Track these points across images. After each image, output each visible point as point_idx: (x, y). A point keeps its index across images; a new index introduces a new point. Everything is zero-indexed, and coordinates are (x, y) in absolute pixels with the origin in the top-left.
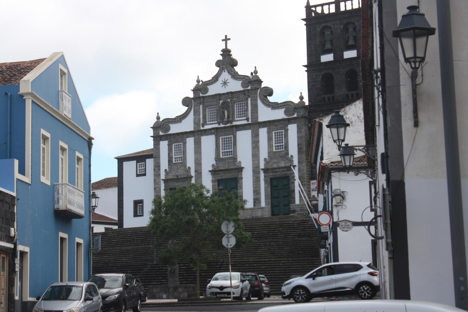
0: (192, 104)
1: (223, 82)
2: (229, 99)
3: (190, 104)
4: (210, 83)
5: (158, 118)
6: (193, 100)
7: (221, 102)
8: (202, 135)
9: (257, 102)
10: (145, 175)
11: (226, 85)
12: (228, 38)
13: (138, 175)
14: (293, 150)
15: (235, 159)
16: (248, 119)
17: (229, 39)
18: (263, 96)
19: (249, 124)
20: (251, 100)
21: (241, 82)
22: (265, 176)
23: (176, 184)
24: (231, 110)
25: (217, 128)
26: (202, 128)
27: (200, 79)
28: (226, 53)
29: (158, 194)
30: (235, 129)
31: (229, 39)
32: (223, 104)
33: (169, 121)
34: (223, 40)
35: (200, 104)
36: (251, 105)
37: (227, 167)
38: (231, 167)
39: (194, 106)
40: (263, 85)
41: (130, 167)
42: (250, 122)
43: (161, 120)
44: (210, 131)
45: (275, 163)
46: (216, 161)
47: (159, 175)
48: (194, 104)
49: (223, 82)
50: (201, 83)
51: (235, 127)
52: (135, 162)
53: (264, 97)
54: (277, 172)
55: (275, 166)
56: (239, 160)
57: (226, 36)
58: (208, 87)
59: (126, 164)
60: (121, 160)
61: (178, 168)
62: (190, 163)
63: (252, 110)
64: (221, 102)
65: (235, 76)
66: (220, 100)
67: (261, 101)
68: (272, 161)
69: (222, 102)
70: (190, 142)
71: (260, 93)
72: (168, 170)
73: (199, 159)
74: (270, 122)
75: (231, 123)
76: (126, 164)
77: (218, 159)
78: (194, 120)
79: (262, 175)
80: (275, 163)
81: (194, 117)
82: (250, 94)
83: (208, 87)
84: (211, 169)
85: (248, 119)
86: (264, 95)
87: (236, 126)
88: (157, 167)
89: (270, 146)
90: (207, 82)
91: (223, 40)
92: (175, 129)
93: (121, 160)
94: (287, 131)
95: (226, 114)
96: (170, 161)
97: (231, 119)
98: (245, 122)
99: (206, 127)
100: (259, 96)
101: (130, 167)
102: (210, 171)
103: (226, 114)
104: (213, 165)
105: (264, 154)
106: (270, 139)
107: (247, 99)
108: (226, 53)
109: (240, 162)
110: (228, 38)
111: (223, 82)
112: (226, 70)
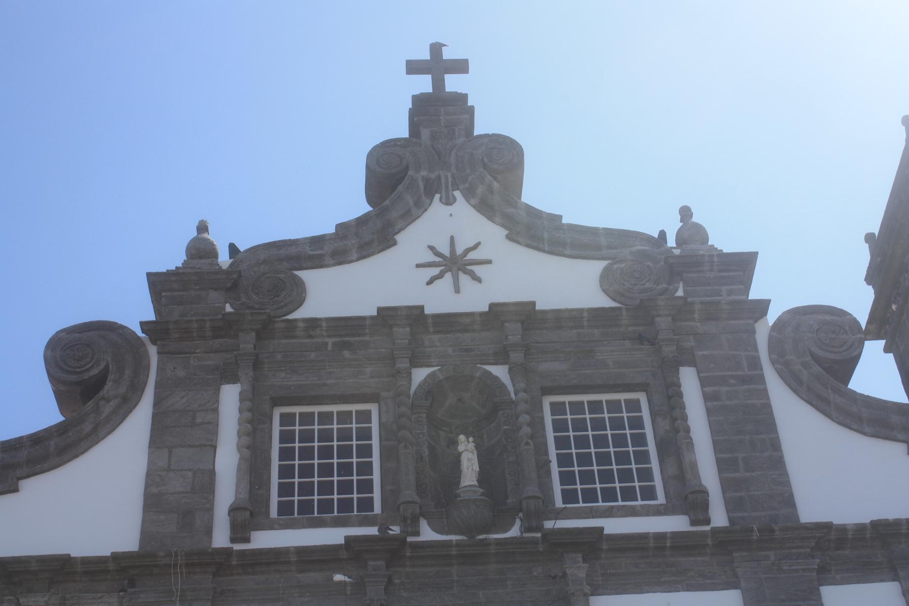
0: (141, 368)
1: (438, 254)
2: (501, 357)
3: (128, 372)
4: (321, 257)
6: (153, 350)
7: (420, 375)
9: (765, 393)
11: (464, 279)
12: (447, 54)
17: (461, 67)
18: (808, 358)
20: (704, 383)
21: (599, 266)
24: (526, 430)
27: (220, 240)
31: (461, 67)
34: (413, 68)
36: (709, 412)
39: (158, 385)
40: (772, 316)
44: (313, 577)
48: (160, 369)
49: (446, 252)
50: (224, 259)
51: (579, 557)
53: (817, 369)
58: (306, 275)
63: (718, 446)
64: (420, 375)
66: (416, 361)
67: (795, 391)
69: (431, 376)
75: (532, 522)
78: (153, 478)
81: (151, 462)
82: (690, 343)
83: (306, 275)
86: (812, 355)
90: (293, 250)
91: (413, 68)
98: (676, 523)
100: (773, 362)
110: (447, 54)
111: (438, 254)
112: (457, 194)
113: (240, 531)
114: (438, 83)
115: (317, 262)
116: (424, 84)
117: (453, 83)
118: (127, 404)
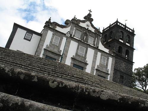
5: (50, 20)
8: (72, 40)
10: (30, 40)
13: (25, 39)
14: (109, 67)
15: (85, 58)
16: (94, 45)
19: (95, 48)
22: (96, 73)
23: (51, 55)
25: (81, 41)
26: (72, 36)
28: (89, 15)
29: (38, 54)
30: (88, 46)
32: (85, 33)
33: (56, 24)
35: (75, 27)
37: (80, 60)
38: (82, 61)
41: (21, 33)
42: (95, 47)
43: (52, 21)
45: (101, 69)
46: (76, 55)
47: (43, 46)
52: (26, 31)
54: (102, 73)
55: (101, 70)
56: (86, 60)
57: (90, 10)
59: (19, 30)
60: (16, 26)
61: (54, 48)
62: (62, 48)
65: (92, 26)
68: (101, 68)
70: (64, 39)
71: (101, 39)
72: (48, 46)
73: (68, 49)
74: (103, 51)
76: (19, 30)
77: (77, 54)
79: (95, 72)
80: (101, 69)
84: (72, 57)
85: (94, 45)
87: (90, 45)
88: (42, 41)
89: (101, 61)
92: (58, 29)
93: (16, 26)
94: (108, 59)
95: (85, 38)
96: (51, 42)
97: (87, 40)
98: (93, 46)
99: (74, 37)
101: (21, 33)
102: (71, 58)
103: (85, 38)
104: (74, 56)
105: (98, 63)
106: (101, 58)
107: (96, 37)
108: (89, 15)
109: (87, 61)
113: (74, 36)
114: (90, 12)
115: (81, 22)
116: (89, 12)
117: (91, 13)
118: (70, 26)
